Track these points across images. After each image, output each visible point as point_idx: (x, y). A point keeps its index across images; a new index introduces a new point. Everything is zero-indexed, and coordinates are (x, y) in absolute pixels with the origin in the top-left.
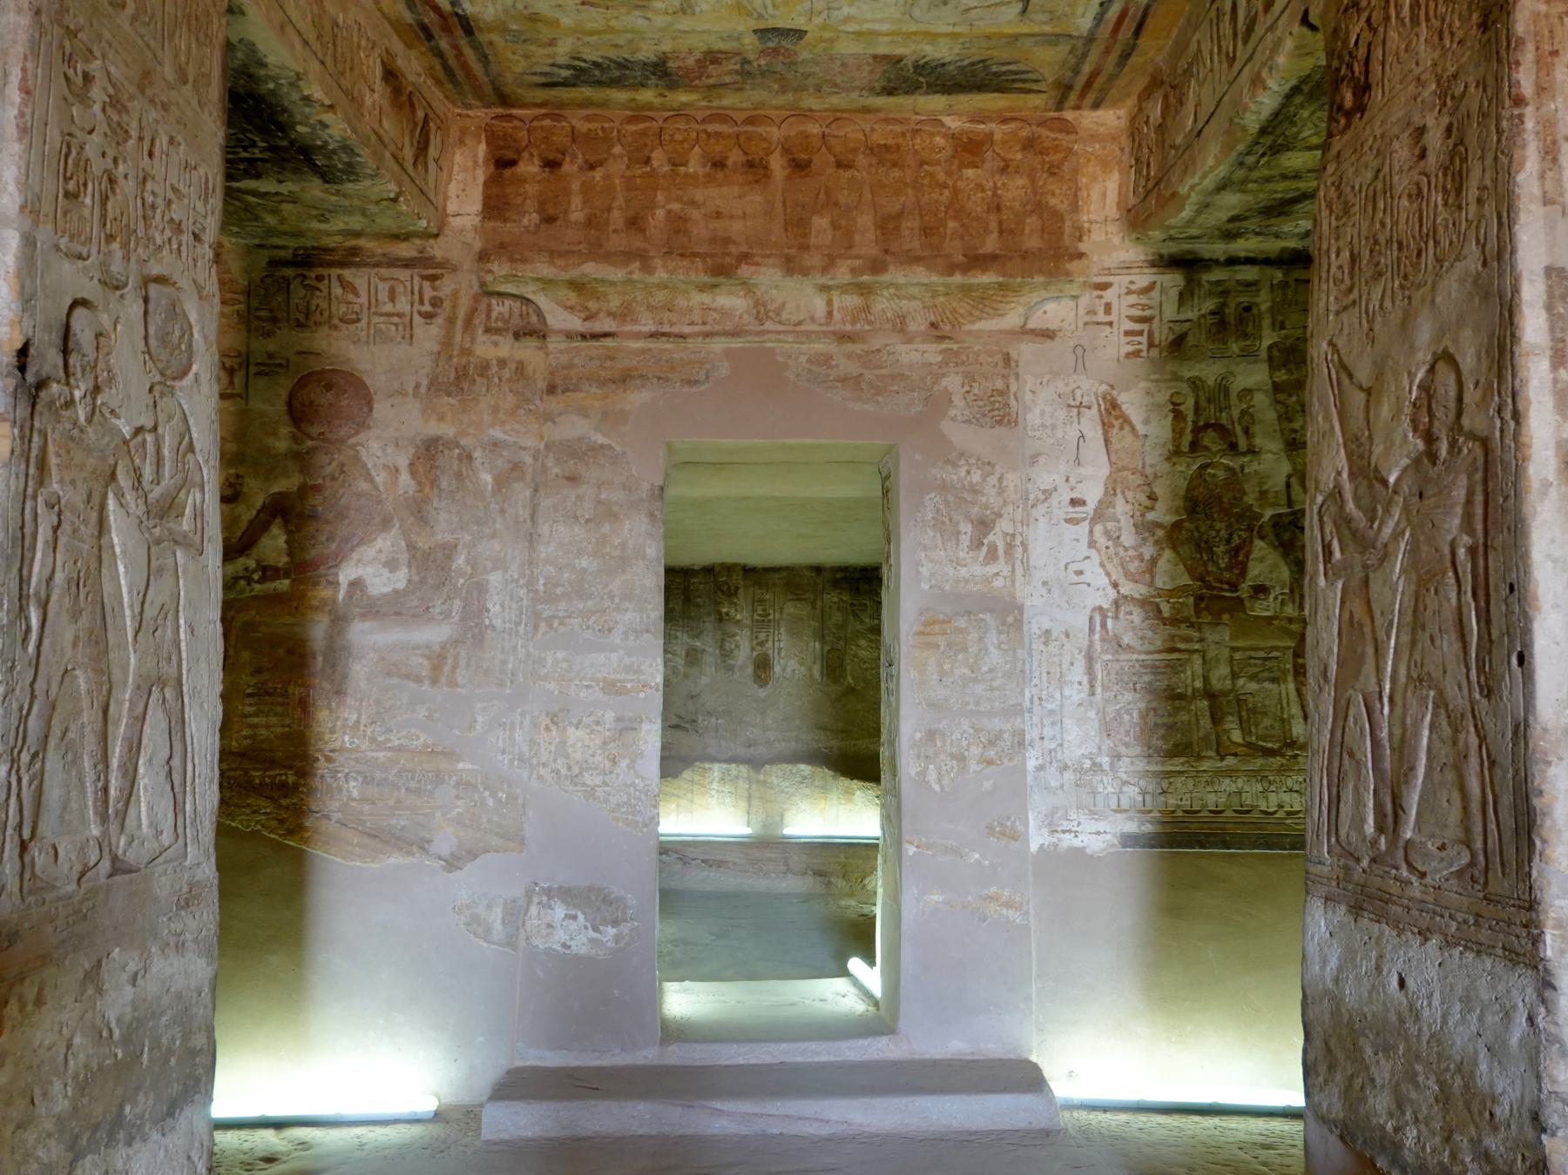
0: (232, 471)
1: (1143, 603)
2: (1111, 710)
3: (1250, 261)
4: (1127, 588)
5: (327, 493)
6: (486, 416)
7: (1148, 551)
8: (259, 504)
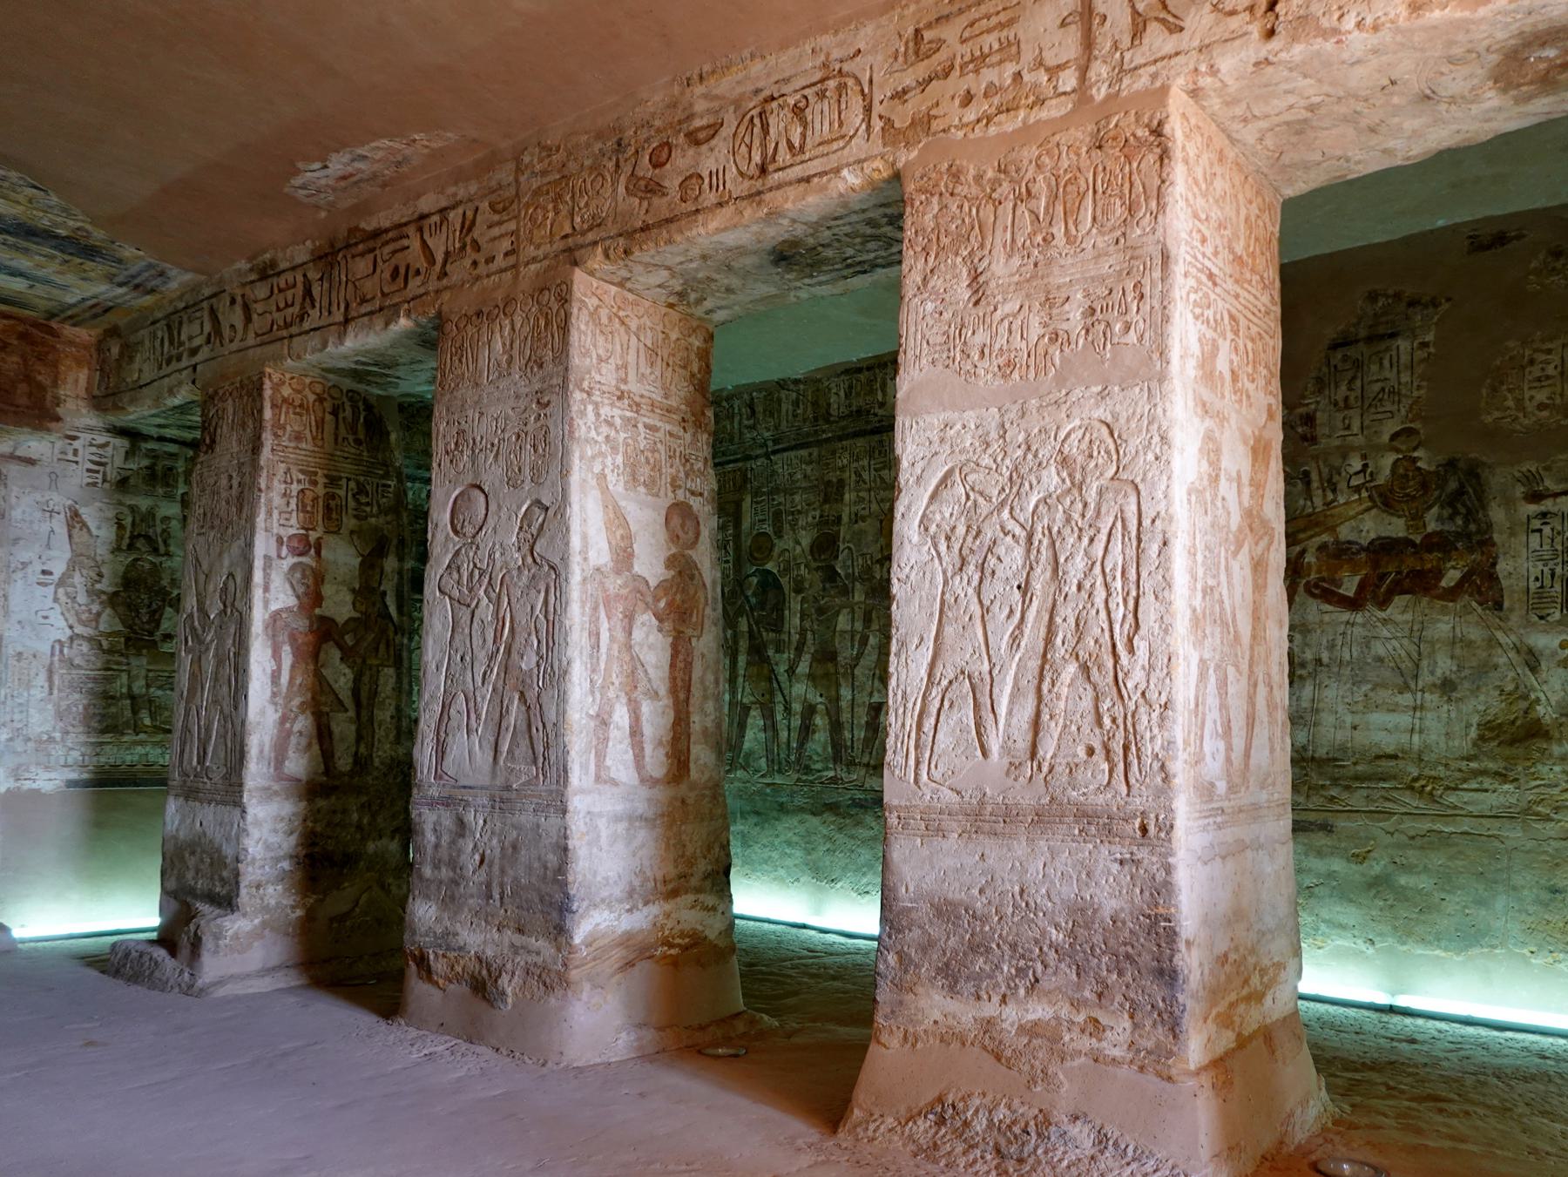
1: (90, 639)
2: (64, 704)
3: (172, 441)
4: (79, 629)
7: (95, 608)
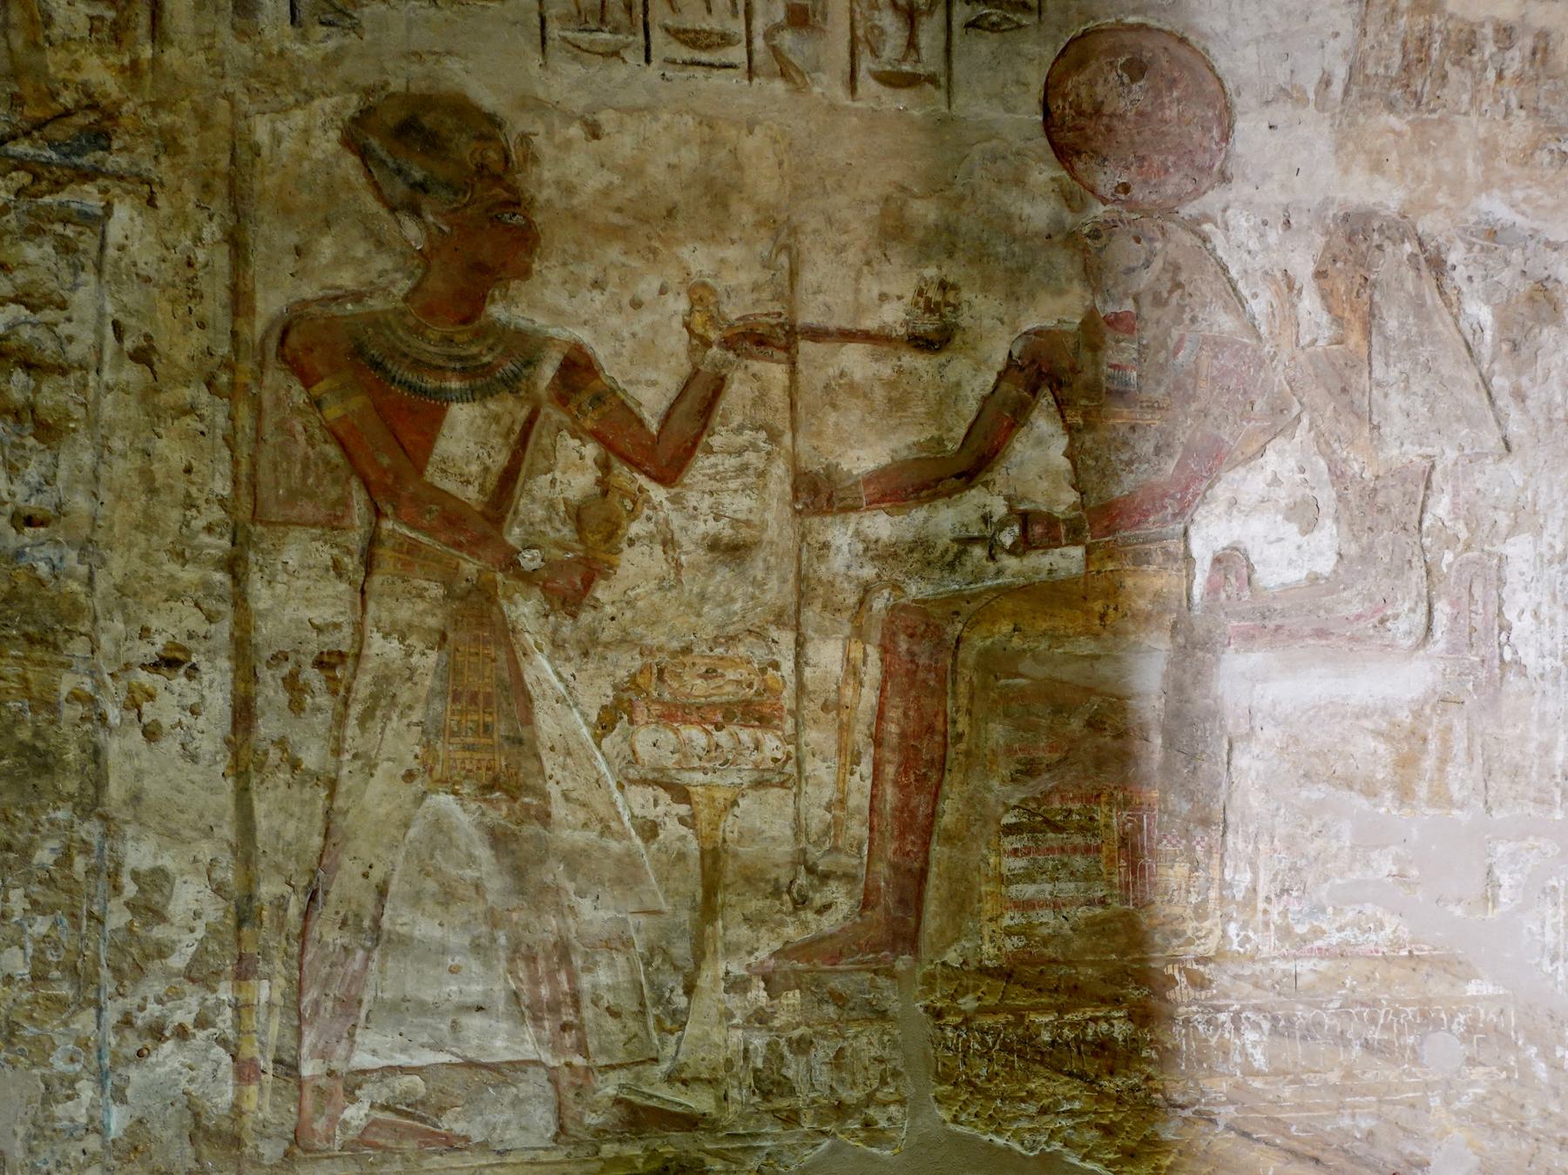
0: (931, 272)
5: (1147, 335)
6: (1470, 164)
8: (999, 359)
